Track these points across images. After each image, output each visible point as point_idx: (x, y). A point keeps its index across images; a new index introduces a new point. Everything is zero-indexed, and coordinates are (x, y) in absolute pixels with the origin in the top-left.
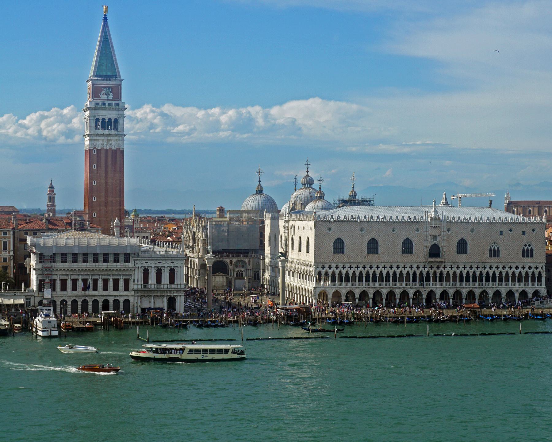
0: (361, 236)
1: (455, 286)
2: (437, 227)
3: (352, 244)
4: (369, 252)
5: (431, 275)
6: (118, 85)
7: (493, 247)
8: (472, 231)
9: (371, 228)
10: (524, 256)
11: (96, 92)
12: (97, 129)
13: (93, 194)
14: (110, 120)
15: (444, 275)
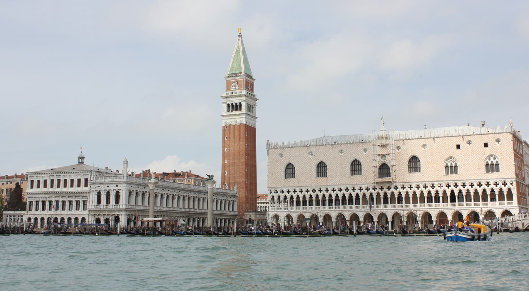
0: (310, 160)
1: (409, 208)
2: (384, 145)
3: (302, 169)
4: (320, 175)
5: (382, 197)
6: (243, 79)
7: (450, 163)
8: (424, 146)
9: (319, 151)
10: (487, 171)
11: (228, 86)
12: (228, 111)
13: (225, 158)
14: (236, 104)
15: (395, 196)
